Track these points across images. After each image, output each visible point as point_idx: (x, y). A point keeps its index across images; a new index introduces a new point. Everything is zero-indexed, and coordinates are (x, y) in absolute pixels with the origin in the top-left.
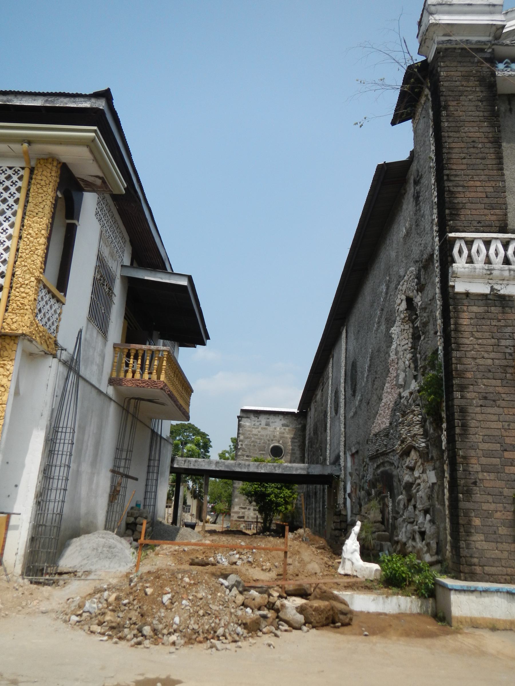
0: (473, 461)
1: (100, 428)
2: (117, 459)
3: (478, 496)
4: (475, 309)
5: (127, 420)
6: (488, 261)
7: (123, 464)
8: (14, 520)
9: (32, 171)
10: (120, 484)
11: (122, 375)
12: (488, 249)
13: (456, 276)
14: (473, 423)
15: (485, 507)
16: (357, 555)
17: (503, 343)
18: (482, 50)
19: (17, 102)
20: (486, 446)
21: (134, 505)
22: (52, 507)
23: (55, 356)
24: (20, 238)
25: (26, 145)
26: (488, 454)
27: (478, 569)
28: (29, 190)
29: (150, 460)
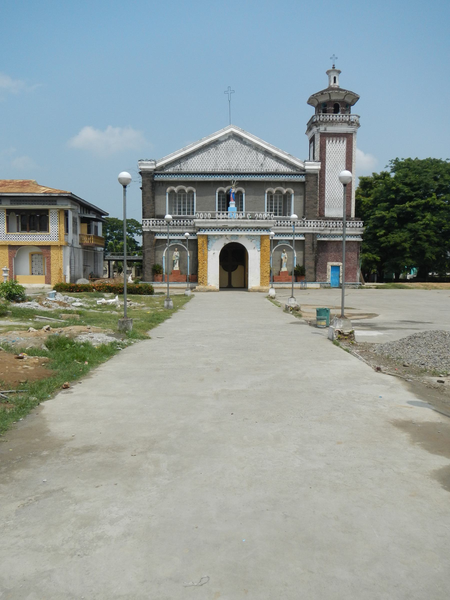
0: (145, 262)
1: (79, 256)
2: (84, 262)
3: (146, 268)
4: (147, 234)
5: (85, 253)
6: (149, 225)
7: (86, 263)
8: (67, 277)
9: (59, 212)
10: (85, 268)
11: (82, 242)
12: (149, 222)
13: (143, 228)
14: (146, 256)
15: (147, 270)
16: (131, 279)
17: (152, 240)
18: (151, 173)
19: (53, 195)
20: (147, 260)
21: (91, 272)
22: (73, 274)
23: (68, 246)
24: (60, 226)
25: (58, 210)
26: (148, 261)
27: (145, 280)
28: (59, 216)
29: (94, 259)
